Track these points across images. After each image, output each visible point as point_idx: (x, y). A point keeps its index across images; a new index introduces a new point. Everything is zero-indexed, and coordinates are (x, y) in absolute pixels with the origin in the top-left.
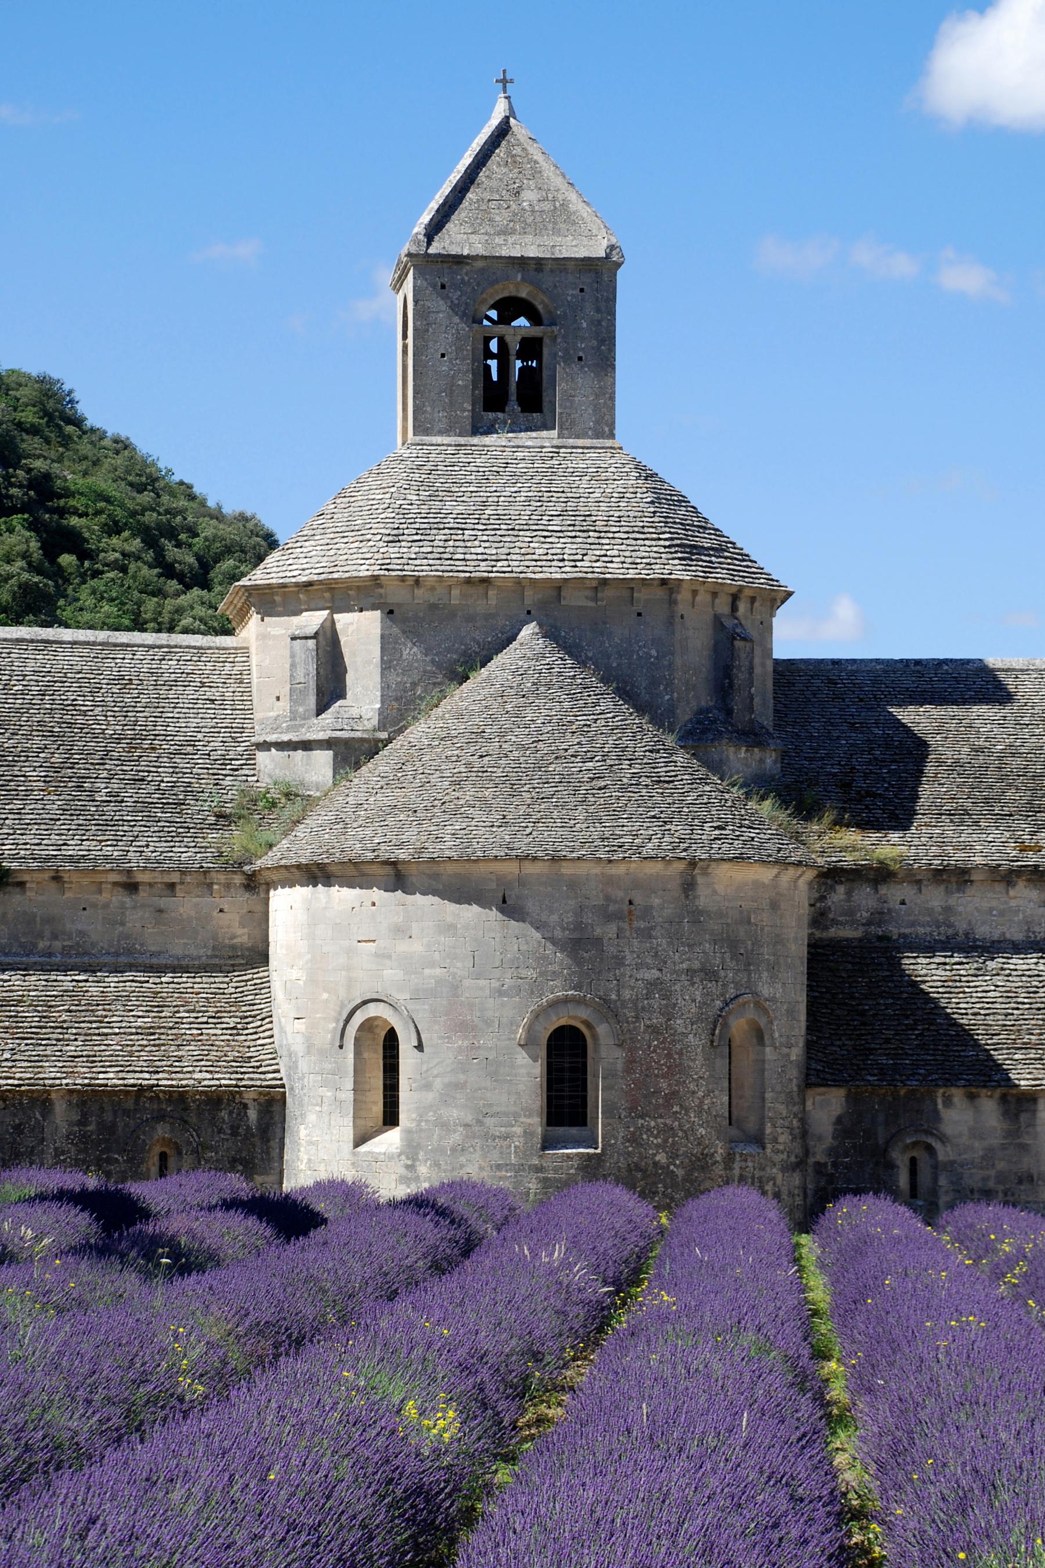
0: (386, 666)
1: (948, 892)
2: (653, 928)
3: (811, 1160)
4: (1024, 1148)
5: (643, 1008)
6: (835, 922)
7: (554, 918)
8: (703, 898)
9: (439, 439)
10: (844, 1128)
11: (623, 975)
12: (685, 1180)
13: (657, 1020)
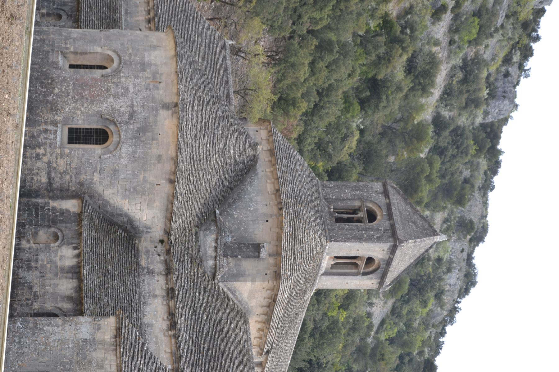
2: (150, 90)
3: (50, 201)
5: (117, 85)
6: (148, 258)
7: (153, 58)
11: (131, 78)
12: (47, 101)
13: (113, 91)
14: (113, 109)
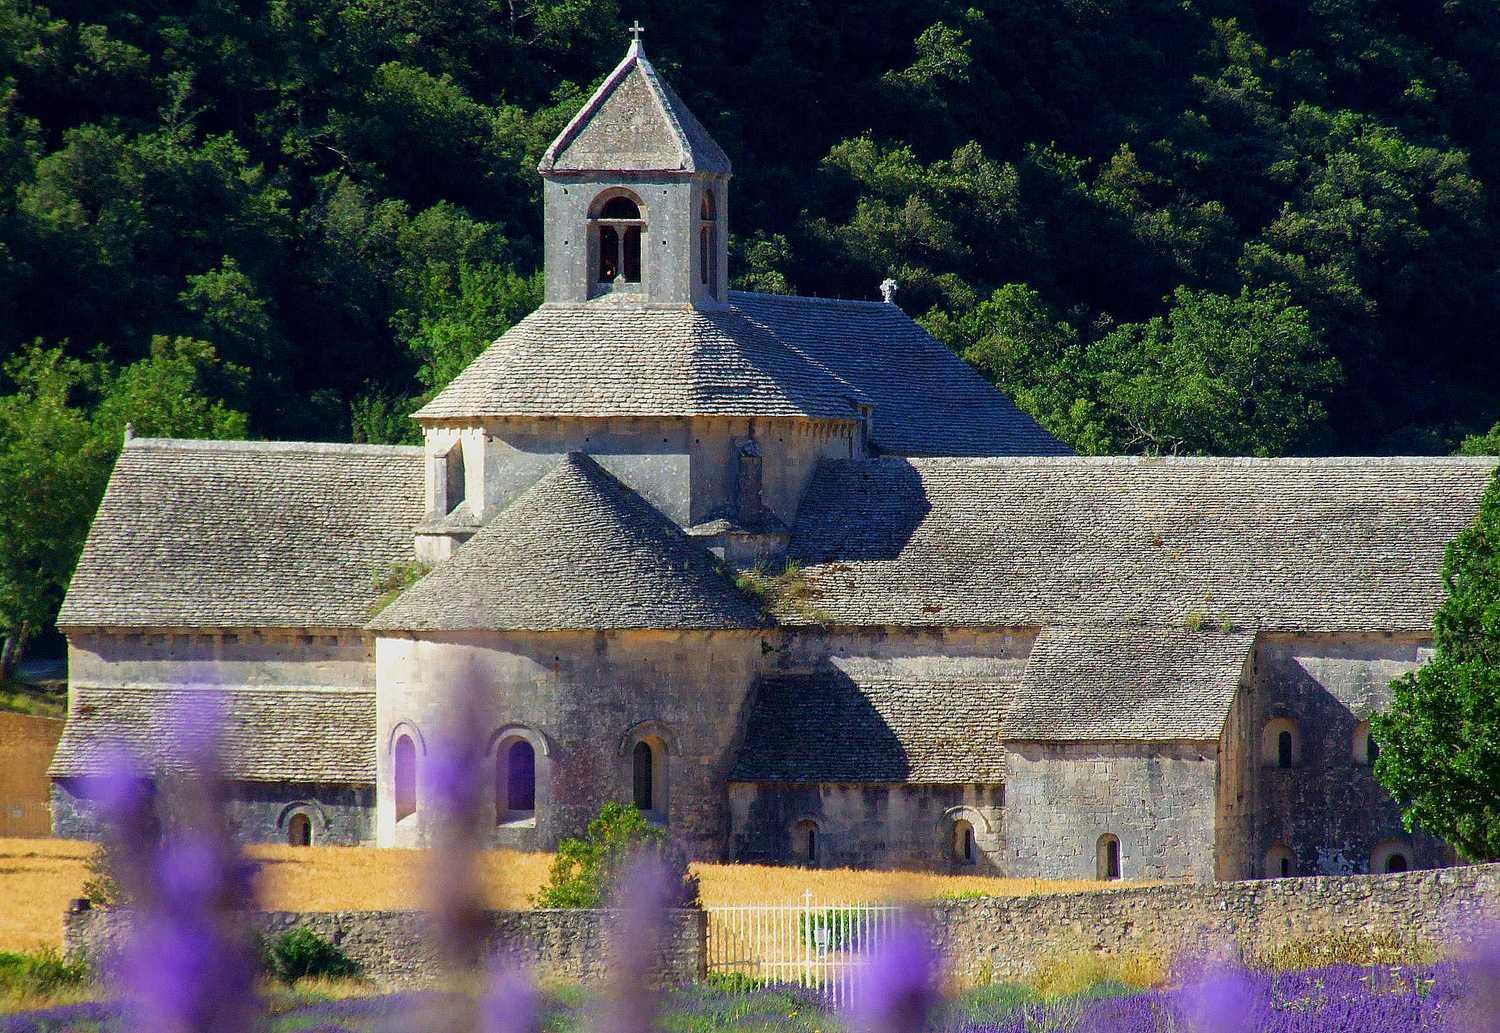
0: (488, 479)
1: (873, 642)
3: (733, 833)
4: (879, 824)
6: (794, 664)
8: (612, 653)
9: (561, 305)
10: (758, 810)
14: (609, 736)
